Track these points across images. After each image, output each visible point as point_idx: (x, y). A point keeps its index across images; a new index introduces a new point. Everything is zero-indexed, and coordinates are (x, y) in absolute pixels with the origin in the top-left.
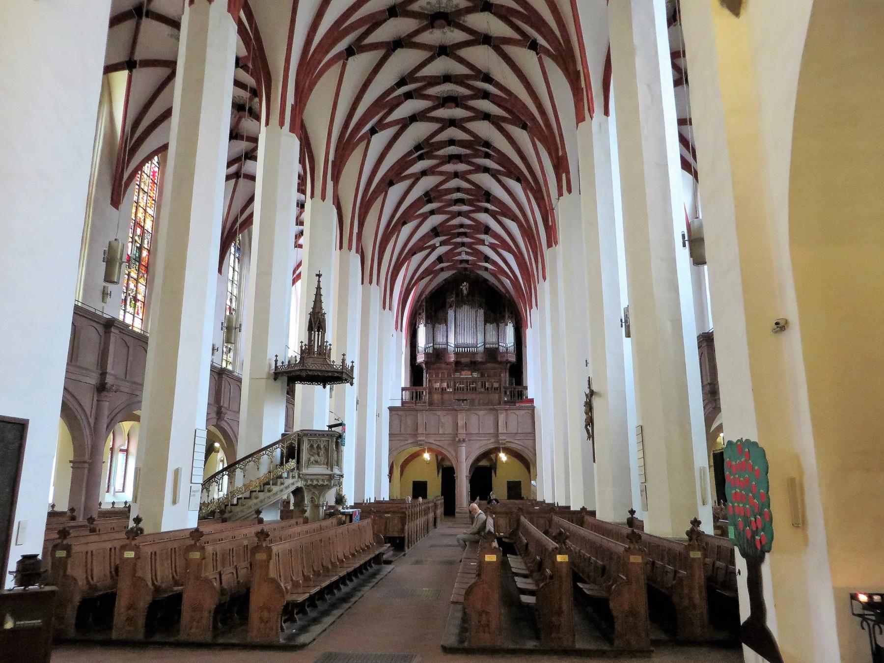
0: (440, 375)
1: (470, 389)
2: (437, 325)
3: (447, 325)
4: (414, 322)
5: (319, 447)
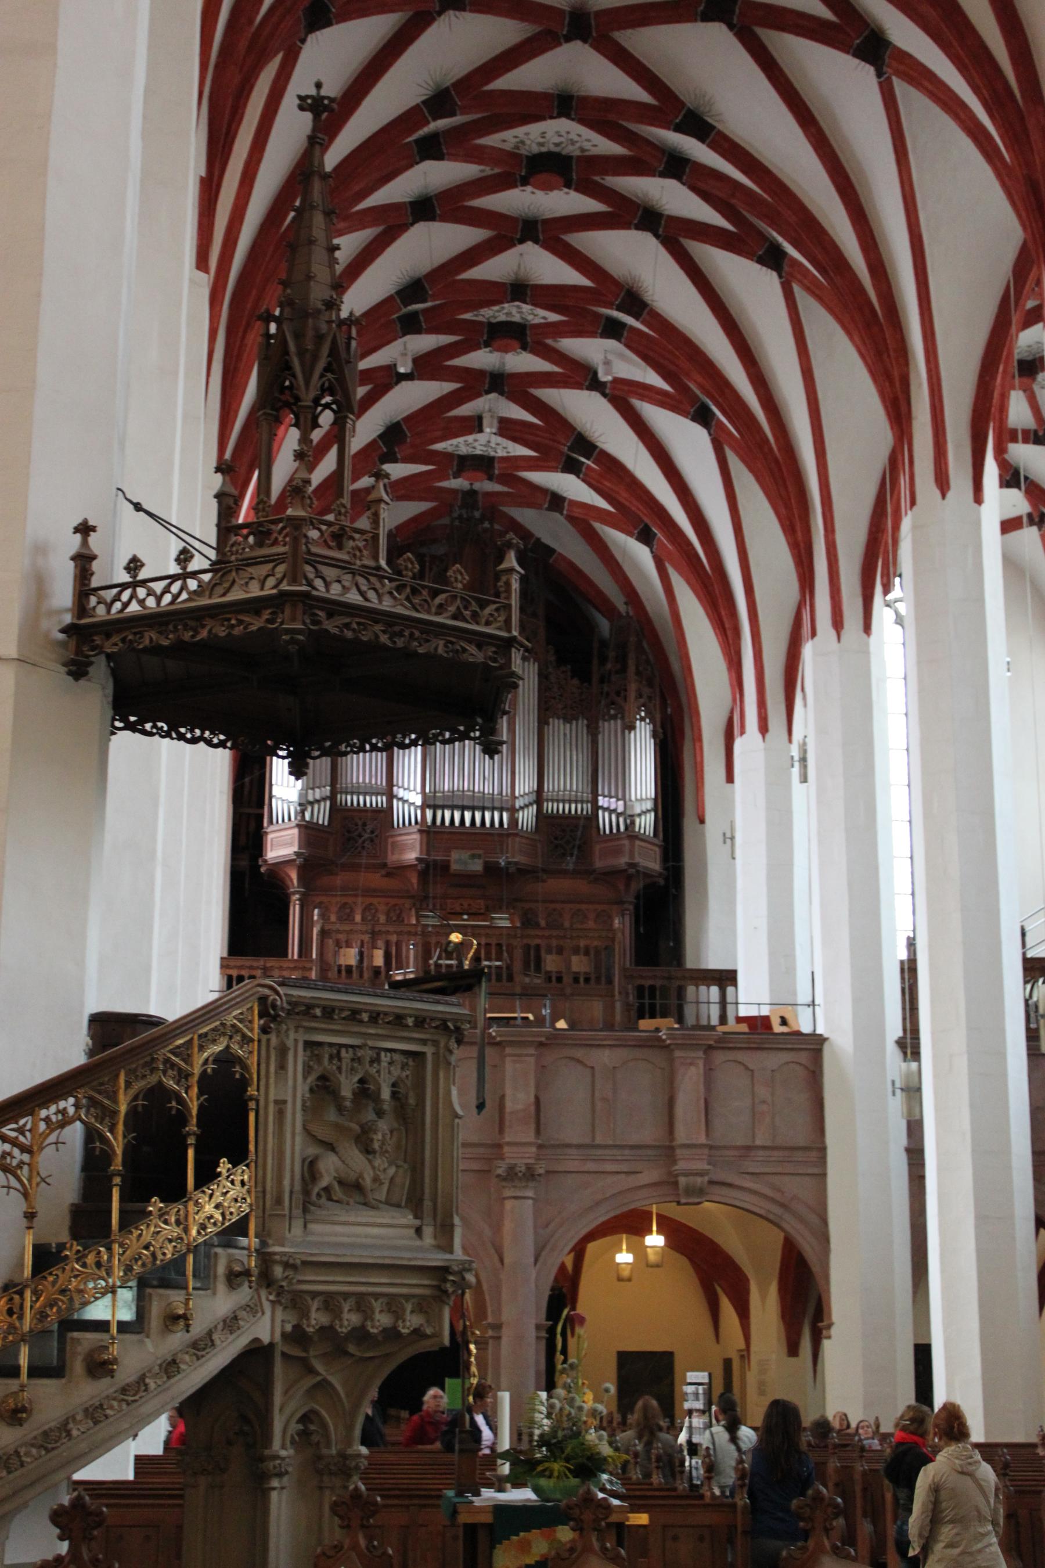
0: (358, 918)
5: (365, 1092)
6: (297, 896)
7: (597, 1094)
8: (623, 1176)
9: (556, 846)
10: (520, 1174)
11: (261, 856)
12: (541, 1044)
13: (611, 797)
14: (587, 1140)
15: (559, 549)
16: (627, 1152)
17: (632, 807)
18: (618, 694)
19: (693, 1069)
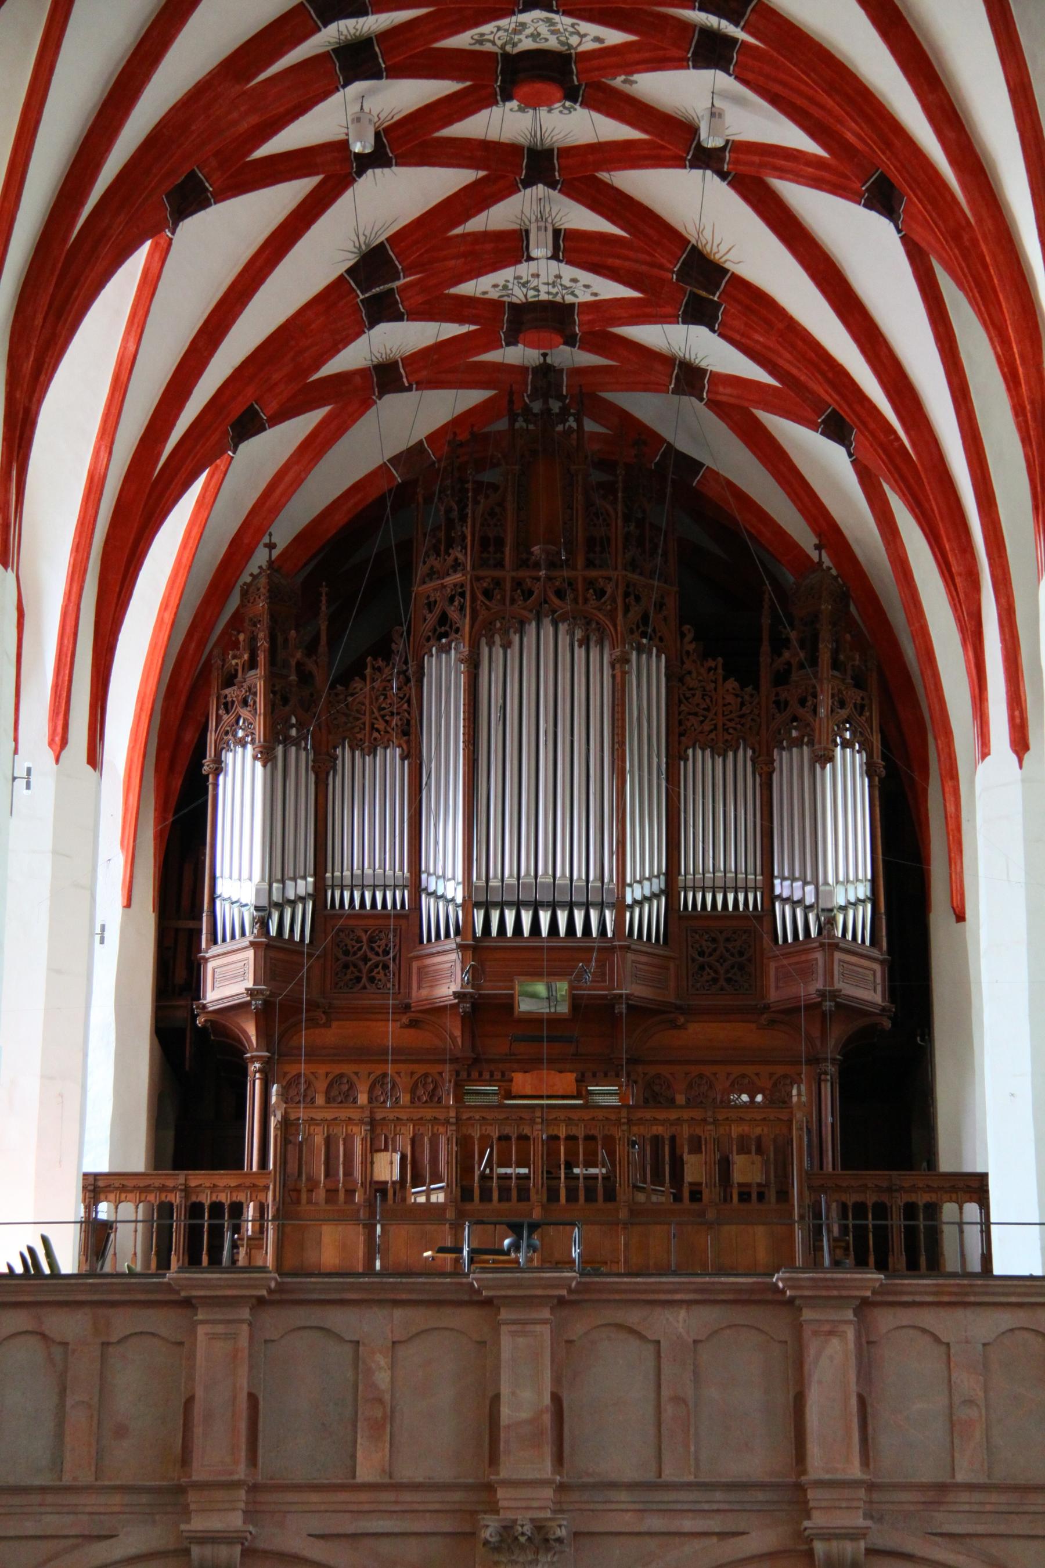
0: (363, 1099)
1: (572, 1196)
2: (344, 754)
3: (413, 756)
4: (189, 736)
6: (257, 1065)
7: (665, 1393)
8: (715, 1540)
9: (702, 968)
10: (523, 1539)
11: (198, 998)
12: (561, 1302)
13: (793, 879)
14: (650, 1476)
15: (708, 462)
16: (719, 1495)
17: (831, 894)
18: (803, 702)
19: (835, 1341)
